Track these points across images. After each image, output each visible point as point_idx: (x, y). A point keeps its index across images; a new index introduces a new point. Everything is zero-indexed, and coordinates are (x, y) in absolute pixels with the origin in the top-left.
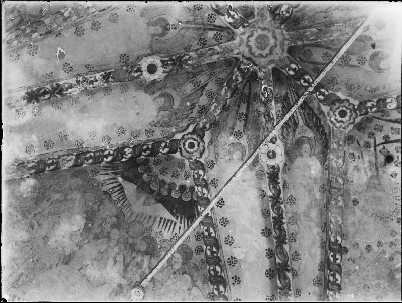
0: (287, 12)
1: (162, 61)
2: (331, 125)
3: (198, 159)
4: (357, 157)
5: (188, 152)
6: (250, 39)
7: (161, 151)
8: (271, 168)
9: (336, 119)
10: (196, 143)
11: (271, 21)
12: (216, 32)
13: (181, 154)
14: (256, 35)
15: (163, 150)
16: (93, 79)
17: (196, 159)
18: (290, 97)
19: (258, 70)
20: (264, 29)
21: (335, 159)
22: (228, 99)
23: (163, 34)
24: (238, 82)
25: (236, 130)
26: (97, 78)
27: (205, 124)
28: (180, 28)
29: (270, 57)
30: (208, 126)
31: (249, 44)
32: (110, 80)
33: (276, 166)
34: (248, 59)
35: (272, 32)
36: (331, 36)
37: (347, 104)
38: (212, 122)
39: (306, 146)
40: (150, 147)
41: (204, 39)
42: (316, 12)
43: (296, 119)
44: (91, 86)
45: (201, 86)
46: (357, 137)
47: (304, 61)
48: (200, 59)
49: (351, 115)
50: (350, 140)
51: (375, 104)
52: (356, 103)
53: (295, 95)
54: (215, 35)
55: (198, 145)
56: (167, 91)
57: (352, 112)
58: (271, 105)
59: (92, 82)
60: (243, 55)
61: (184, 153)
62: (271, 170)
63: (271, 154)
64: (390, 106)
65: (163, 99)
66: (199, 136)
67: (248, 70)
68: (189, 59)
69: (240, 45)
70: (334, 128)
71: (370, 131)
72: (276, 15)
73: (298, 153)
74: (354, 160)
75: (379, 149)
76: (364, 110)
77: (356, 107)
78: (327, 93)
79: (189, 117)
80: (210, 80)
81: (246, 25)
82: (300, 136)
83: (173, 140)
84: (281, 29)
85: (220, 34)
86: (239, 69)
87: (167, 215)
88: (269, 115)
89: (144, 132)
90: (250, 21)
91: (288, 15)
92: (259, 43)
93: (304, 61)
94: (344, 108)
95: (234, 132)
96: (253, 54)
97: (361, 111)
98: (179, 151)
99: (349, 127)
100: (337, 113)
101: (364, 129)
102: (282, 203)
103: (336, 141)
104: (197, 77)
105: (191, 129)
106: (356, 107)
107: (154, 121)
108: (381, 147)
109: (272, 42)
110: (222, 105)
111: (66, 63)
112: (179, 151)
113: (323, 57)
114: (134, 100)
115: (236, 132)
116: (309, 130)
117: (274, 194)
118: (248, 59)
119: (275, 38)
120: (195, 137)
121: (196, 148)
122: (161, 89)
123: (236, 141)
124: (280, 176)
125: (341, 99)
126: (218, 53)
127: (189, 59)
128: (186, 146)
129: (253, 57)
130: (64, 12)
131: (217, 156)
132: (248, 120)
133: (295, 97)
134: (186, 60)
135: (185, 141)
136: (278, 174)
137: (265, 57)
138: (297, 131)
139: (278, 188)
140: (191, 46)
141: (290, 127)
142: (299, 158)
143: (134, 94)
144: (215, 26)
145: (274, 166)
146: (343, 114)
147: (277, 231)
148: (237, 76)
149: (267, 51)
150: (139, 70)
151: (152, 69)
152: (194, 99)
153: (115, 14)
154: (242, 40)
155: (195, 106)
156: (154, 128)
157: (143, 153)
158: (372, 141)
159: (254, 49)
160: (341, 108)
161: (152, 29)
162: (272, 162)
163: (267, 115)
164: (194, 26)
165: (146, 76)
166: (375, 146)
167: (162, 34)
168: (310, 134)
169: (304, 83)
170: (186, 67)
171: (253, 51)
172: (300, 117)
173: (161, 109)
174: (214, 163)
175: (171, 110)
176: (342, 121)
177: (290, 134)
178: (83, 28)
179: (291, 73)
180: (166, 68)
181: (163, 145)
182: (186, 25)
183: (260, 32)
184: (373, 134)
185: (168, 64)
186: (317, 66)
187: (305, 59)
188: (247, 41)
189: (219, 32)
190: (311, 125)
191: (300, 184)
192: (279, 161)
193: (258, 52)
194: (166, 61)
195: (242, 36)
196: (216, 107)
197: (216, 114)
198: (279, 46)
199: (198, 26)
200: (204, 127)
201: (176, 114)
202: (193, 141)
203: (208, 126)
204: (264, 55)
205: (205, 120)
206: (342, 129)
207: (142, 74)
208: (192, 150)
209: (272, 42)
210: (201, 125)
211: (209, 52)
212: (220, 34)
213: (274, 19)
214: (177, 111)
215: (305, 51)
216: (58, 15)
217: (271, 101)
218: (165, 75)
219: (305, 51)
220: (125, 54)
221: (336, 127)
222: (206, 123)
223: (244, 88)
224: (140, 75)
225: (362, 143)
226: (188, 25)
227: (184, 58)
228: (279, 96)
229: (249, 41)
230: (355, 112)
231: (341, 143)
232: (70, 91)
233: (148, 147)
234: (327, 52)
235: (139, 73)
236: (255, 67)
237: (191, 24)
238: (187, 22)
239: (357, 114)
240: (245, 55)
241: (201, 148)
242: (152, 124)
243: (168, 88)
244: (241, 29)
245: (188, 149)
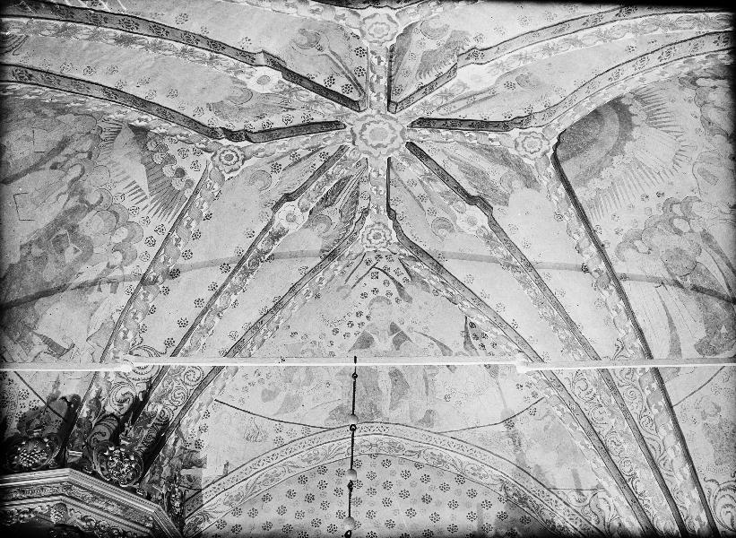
3: (223, 172)
5: (220, 160)
10: (235, 158)
13: (212, 158)
25: (279, 162)
28: (324, 53)
31: (367, 126)
34: (354, 134)
75: (373, 270)
87: (143, 182)
108: (377, 270)
120: (239, 153)
121: (232, 162)
129: (358, 136)
144: (355, 79)
156: (206, 111)
158: (375, 262)
160: (380, 232)
162: (285, 224)
166: (373, 267)
176: (370, 241)
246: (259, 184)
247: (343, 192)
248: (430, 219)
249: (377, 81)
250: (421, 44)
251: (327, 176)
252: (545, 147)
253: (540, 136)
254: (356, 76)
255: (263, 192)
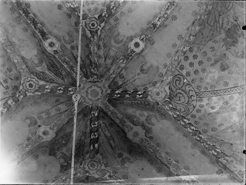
0: (93, 114)
1: (135, 52)
2: (33, 76)
3: (86, 20)
4: (7, 72)
5: (93, 21)
6: (101, 91)
7: (106, 13)
8: (47, 38)
9: (32, 81)
10: (92, 27)
11: (98, 105)
12: (119, 85)
14: (100, 94)
15: (105, 14)
16: (160, 20)
17: (87, 19)
18: (61, 81)
19: (87, 80)
20: (98, 100)
21: (19, 60)
22: (91, 58)
23: (142, 67)
24: (92, 68)
26: (159, 22)
27: (94, 39)
28: (136, 76)
29: (86, 89)
30: (92, 39)
31: (100, 89)
32: (152, 26)
33: (46, 40)
34: (95, 82)
35: (94, 101)
36: (65, 116)
37: (32, 91)
38: (91, 42)
39: (36, 62)
40: (112, 10)
41: (122, 78)
42: (79, 125)
43: (51, 72)
44: (159, 17)
45: (107, 58)
46: (14, 81)
47: (67, 101)
48: (118, 66)
49: (26, 87)
50: (17, 78)
51: (19, 98)
52: (28, 94)
53: (59, 83)
54: (118, 84)
55: (90, 27)
56: (122, 44)
57: (27, 89)
58: (69, 68)
59: (160, 18)
60: (99, 82)
61: (94, 19)
62: (47, 37)
63: (52, 45)
64: (11, 101)
65: (121, 39)
66: (93, 32)
67: (92, 77)
68: (123, 62)
69: (104, 85)
70: (30, 76)
71: (9, 89)
72: (98, 108)
73: (38, 56)
74: (8, 69)
76: (22, 93)
77: (27, 92)
78: (46, 90)
79: (103, 40)
80: (105, 63)
81: (108, 95)
82: (43, 65)
83: (104, 21)
84: (91, 105)
85: (116, 86)
86: (96, 75)
88: (66, 63)
89: (119, 18)
90: (107, 98)
91: (92, 112)
92: (96, 92)
93: (67, 101)
94: (32, 88)
95: (76, 48)
96: (94, 86)
97: (23, 92)
98: (98, 18)
99: (23, 81)
100: (34, 84)
101: (13, 89)
102: (31, 23)
103: (25, 70)
104: (112, 60)
105: (99, 32)
106: (27, 92)
107: (118, 26)
109: (90, 97)
110: (92, 53)
111: (176, 20)
112: (98, 18)
113: (60, 108)
114: (134, 29)
115: (75, 48)
116: (41, 70)
117: (37, 25)
118: (95, 82)
119: (90, 99)
120: (94, 30)
121: (90, 25)
122: (125, 43)
123: (72, 44)
124: (41, 37)
125: (37, 92)
126: (111, 74)
127: (123, 62)
128: (95, 23)
129: (94, 84)
130: (193, 38)
131: (76, 30)
132: (73, 58)
133: (59, 82)
134: (124, 61)
135: (97, 25)
136: (42, 37)
137: (88, 88)
138: (46, 67)
139: (37, 30)
140: (125, 71)
141: (51, 67)
142: (36, 53)
143: (136, 31)
144: (121, 88)
145: (47, 40)
146: (31, 86)
147: (24, 7)
148: (95, 71)
149: (89, 92)
150: (142, 40)
151: (137, 45)
152: (106, 50)
153: (170, 58)
154: (105, 88)
155: (103, 47)
156: (115, 23)
157: (113, 5)
159: (96, 88)
160: (34, 87)
161: (149, 65)
162: (49, 41)
163: (67, 62)
164: (130, 81)
165: (138, 40)
167: (143, 67)
168: (39, 69)
169: (61, 89)
170: (122, 58)
171: (96, 86)
172: (50, 74)
173: (119, 34)
174: (75, 26)
175: (113, 37)
177: (48, 63)
178: (179, 40)
179: (70, 89)
180: (131, 50)
181: (107, 16)
182: (134, 79)
183: (99, 97)
184: (6, 89)
185: (131, 52)
186: (59, 103)
187: (68, 102)
188: (102, 89)
189: (117, 86)
190: (42, 74)
191: (27, 41)
192: (46, 44)
193: (93, 88)
194: (133, 53)
195: (106, 89)
196: (94, 50)
197: (92, 47)
198: (86, 97)
199: (128, 82)
200: (93, 37)
201: (110, 37)
202: (94, 27)
203: (92, 39)
204: (89, 89)
205: (95, 41)
206: (26, 78)
207: (140, 39)
208: (91, 23)
209: (90, 97)
210: (95, 37)
211: (116, 72)
212: (116, 86)
213: (97, 107)
214: (110, 39)
215: (70, 105)
216: (195, 34)
217: (70, 70)
218: (129, 47)
219: (70, 105)
220: (153, 44)
221: (29, 77)
222: (94, 40)
223: (86, 70)
224: (140, 38)
225: (9, 81)
226: (133, 80)
227: (126, 61)
228: (67, 77)
229: (101, 89)
230: (25, 90)
231: (22, 70)
232: (167, 7)
233: (113, 9)
234: (59, 111)
235: (141, 38)
236: (89, 80)
237: (132, 81)
238: (135, 80)
239: (24, 89)
240: (99, 83)
241: (88, 27)
242: (117, 24)
243: (122, 45)
244: (109, 92)
245: (94, 22)
246: (67, 38)
247: (55, 75)
248: (35, 116)
249: (128, 94)
250: (142, 115)
251: (73, 67)
252: (91, 172)
253: (99, 168)
254: (123, 88)
255: (62, 38)
